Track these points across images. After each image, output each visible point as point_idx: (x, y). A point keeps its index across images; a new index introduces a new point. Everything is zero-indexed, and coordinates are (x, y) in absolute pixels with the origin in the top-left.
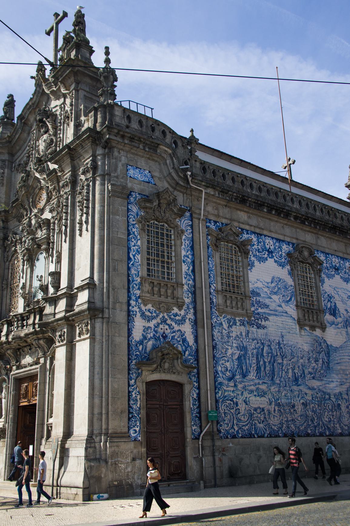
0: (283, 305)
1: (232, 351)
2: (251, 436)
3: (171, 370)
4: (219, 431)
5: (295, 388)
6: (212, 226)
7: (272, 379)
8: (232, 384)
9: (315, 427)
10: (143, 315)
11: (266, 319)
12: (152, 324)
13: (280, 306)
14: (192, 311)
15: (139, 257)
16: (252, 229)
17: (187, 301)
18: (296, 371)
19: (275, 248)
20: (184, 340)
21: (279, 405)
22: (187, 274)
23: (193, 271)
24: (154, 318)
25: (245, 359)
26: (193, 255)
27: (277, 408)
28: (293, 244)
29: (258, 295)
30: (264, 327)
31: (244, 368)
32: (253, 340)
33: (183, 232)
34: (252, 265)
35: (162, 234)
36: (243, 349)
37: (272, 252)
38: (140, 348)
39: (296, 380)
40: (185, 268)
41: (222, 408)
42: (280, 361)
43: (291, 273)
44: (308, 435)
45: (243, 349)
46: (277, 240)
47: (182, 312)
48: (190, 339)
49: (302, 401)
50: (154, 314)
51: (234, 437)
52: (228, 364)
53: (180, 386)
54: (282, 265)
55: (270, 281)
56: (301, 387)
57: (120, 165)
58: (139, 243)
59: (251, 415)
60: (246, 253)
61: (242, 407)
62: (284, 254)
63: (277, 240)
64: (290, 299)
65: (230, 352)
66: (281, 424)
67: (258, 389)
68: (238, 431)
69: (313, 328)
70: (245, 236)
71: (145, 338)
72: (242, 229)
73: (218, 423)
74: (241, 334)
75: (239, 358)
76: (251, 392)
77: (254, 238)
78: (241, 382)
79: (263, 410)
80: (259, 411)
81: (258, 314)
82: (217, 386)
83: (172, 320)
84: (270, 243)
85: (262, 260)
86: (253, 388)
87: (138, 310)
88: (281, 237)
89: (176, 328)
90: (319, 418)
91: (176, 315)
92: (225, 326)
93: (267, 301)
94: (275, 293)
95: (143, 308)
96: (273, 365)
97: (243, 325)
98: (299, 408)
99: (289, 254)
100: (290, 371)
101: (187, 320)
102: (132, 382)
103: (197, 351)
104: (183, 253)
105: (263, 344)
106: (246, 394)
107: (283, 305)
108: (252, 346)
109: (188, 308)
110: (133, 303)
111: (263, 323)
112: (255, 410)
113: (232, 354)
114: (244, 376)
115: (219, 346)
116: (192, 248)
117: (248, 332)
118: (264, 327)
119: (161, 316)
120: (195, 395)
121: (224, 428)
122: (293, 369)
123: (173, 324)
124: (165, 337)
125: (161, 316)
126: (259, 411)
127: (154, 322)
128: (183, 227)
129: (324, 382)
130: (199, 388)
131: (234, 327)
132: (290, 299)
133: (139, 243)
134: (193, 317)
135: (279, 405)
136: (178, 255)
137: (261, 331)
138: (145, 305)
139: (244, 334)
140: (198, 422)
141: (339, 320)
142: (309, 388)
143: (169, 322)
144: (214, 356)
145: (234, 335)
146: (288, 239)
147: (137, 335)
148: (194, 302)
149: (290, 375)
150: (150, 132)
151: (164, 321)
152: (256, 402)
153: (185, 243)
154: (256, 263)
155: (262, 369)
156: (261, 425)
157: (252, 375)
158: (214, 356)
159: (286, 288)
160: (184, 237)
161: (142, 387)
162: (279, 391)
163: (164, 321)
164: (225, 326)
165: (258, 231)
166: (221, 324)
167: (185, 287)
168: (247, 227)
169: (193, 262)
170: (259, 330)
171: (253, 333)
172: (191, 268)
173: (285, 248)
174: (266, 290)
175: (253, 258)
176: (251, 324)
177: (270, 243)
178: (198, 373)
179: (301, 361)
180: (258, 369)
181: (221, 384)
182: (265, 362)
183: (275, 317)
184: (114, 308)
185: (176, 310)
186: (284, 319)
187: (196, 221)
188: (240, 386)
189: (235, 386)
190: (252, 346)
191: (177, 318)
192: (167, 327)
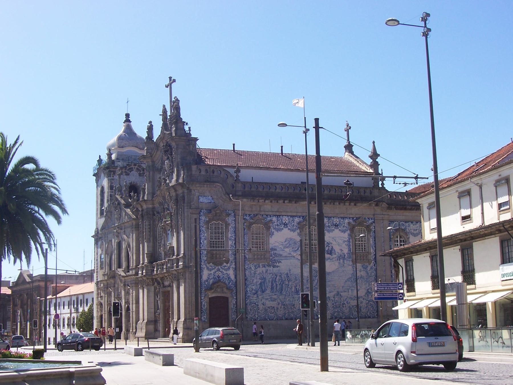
0: (292, 253)
1: (257, 280)
2: (266, 319)
3: (222, 292)
4: (247, 318)
5: (296, 296)
6: (248, 218)
7: (281, 293)
8: (255, 296)
10: (208, 268)
11: (280, 262)
12: (212, 272)
14: (234, 263)
15: (206, 241)
16: (274, 213)
18: (297, 287)
19: (289, 222)
20: (229, 278)
22: (231, 246)
23: (235, 244)
24: (213, 269)
25: (264, 284)
26: (235, 235)
27: (282, 307)
28: (303, 217)
29: (275, 250)
31: (263, 288)
32: (270, 274)
33: (229, 224)
34: (273, 234)
35: (219, 228)
37: (287, 224)
38: (207, 283)
40: (230, 243)
41: (249, 307)
42: (287, 283)
43: (299, 235)
46: (291, 216)
47: (229, 265)
48: (232, 277)
52: (254, 287)
53: (227, 299)
54: (294, 231)
57: (195, 198)
58: (206, 235)
59: (266, 310)
60: (268, 228)
61: (261, 307)
62: (295, 224)
63: (291, 216)
64: (298, 249)
65: (255, 281)
68: (257, 318)
70: (269, 218)
71: (209, 278)
72: (267, 215)
73: (246, 314)
74: (263, 272)
75: (261, 284)
76: (267, 299)
77: (274, 219)
78: (260, 295)
79: (274, 307)
82: (246, 297)
84: (285, 219)
85: (279, 230)
88: (295, 214)
89: (225, 272)
91: (225, 266)
92: (253, 268)
93: (281, 253)
95: (208, 266)
96: (282, 285)
97: (264, 267)
99: (299, 223)
100: (293, 288)
101: (231, 268)
102: (202, 298)
103: (236, 282)
104: (230, 235)
106: (263, 301)
107: (292, 253)
108: (269, 277)
109: (232, 262)
110: (202, 263)
111: (278, 264)
112: (269, 307)
113: (256, 282)
114: (263, 292)
115: (249, 279)
116: (235, 232)
117: (267, 270)
119: (217, 268)
120: (234, 302)
121: (249, 316)
122: (295, 287)
123: (223, 271)
124: (219, 277)
125: (217, 268)
127: (213, 271)
128: (230, 222)
130: (236, 299)
131: (258, 268)
132: (298, 249)
133: (206, 235)
134: (234, 266)
136: (227, 238)
138: (209, 264)
139: (264, 272)
140: (236, 314)
141: (334, 256)
143: (221, 270)
144: (246, 284)
146: (299, 214)
147: (205, 277)
148: (235, 258)
149: (293, 289)
150: (212, 174)
151: (219, 270)
152: (269, 304)
153: (231, 229)
154: (275, 233)
155: (275, 288)
156: (272, 315)
157: (268, 291)
158: (246, 284)
159: (295, 243)
160: (230, 227)
161: (207, 300)
162: (285, 298)
164: (253, 268)
165: (278, 214)
166: (251, 268)
167: (230, 252)
168: (270, 213)
169: (235, 239)
171: (270, 270)
172: (234, 242)
173: (297, 220)
175: (273, 230)
176: (269, 266)
177: (285, 219)
178: (236, 292)
180: (272, 288)
181: (249, 296)
182: (277, 285)
183: (286, 261)
185: (225, 264)
186: (291, 261)
187: (237, 217)
188: (260, 297)
190: (269, 277)
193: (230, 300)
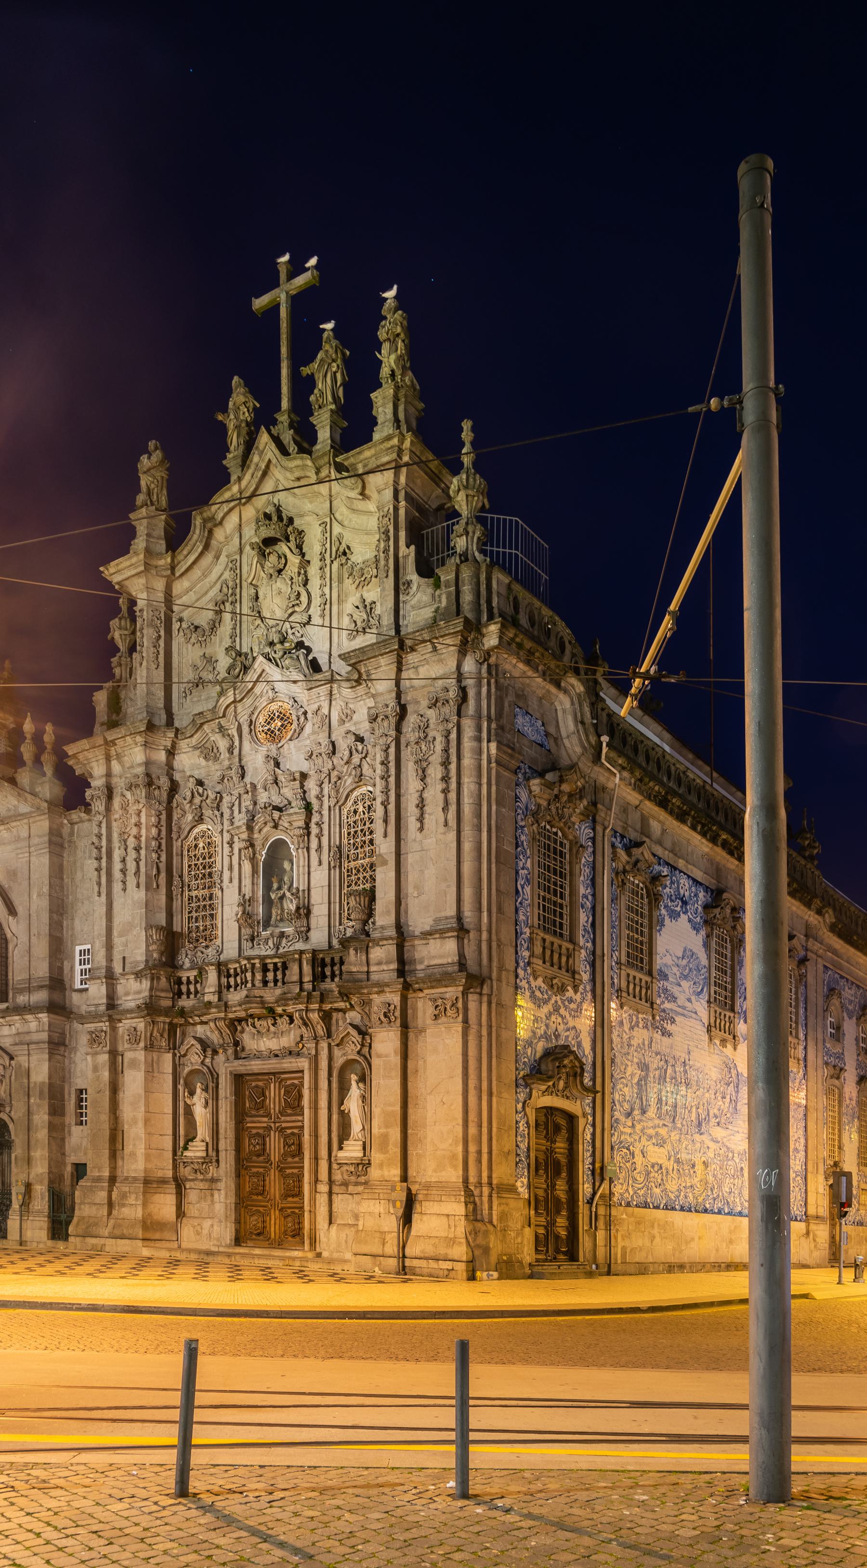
0: (693, 998)
2: (646, 1206)
5: (697, 1137)
9: (715, 1199)
11: (673, 1021)
13: (689, 1000)
17: (586, 977)
18: (700, 1111)
21: (678, 1161)
24: (546, 1002)
30: (670, 1035)
32: (657, 1054)
36: (644, 1067)
38: (529, 1051)
39: (700, 1124)
43: (706, 945)
44: (706, 1211)
45: (644, 1067)
47: (578, 997)
49: (703, 1159)
50: (546, 996)
51: (628, 1205)
55: (680, 954)
56: (703, 1137)
61: (639, 1159)
65: (629, 1070)
66: (679, 1191)
67: (657, 1134)
69: (723, 1042)
76: (651, 1137)
80: (656, 1168)
81: (664, 1011)
83: (566, 1007)
86: (651, 1132)
87: (527, 986)
90: (720, 1187)
92: (626, 1027)
94: (686, 977)
95: (533, 984)
98: (699, 1168)
100: (694, 1109)
105: (666, 1061)
113: (632, 1075)
114: (644, 1112)
115: (618, 1060)
118: (670, 1035)
119: (553, 1001)
126: (656, 1168)
129: (729, 1132)
130: (594, 1125)
135: (678, 1161)
137: (665, 1039)
138: (535, 978)
139: (646, 1043)
142: (712, 1140)
143: (562, 1011)
145: (634, 1042)
148: (593, 980)
152: (657, 1155)
156: (657, 1191)
157: (652, 1112)
162: (680, 1140)
163: (556, 1009)
170: (664, 1039)
174: (675, 969)
175: (663, 912)
179: (707, 1095)
184: (499, 980)
188: (638, 1127)
189: (633, 1126)
191: (573, 1006)
192: (560, 1020)
193: (582, 1122)
